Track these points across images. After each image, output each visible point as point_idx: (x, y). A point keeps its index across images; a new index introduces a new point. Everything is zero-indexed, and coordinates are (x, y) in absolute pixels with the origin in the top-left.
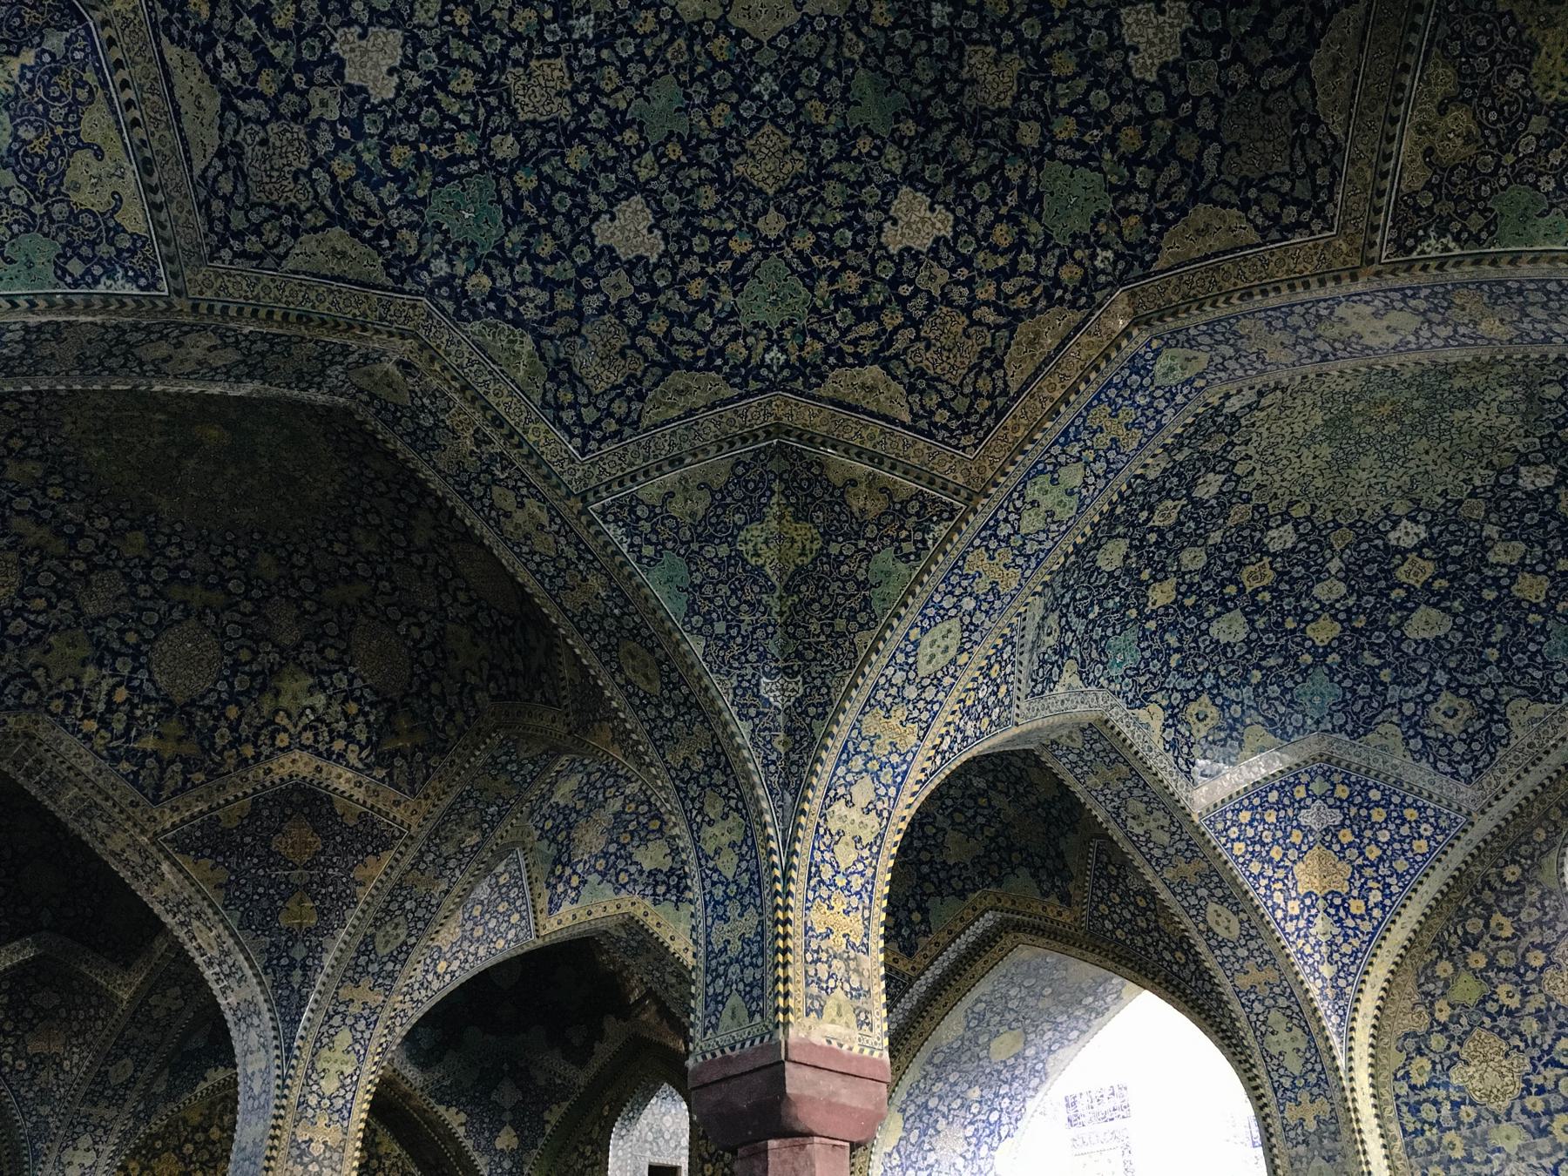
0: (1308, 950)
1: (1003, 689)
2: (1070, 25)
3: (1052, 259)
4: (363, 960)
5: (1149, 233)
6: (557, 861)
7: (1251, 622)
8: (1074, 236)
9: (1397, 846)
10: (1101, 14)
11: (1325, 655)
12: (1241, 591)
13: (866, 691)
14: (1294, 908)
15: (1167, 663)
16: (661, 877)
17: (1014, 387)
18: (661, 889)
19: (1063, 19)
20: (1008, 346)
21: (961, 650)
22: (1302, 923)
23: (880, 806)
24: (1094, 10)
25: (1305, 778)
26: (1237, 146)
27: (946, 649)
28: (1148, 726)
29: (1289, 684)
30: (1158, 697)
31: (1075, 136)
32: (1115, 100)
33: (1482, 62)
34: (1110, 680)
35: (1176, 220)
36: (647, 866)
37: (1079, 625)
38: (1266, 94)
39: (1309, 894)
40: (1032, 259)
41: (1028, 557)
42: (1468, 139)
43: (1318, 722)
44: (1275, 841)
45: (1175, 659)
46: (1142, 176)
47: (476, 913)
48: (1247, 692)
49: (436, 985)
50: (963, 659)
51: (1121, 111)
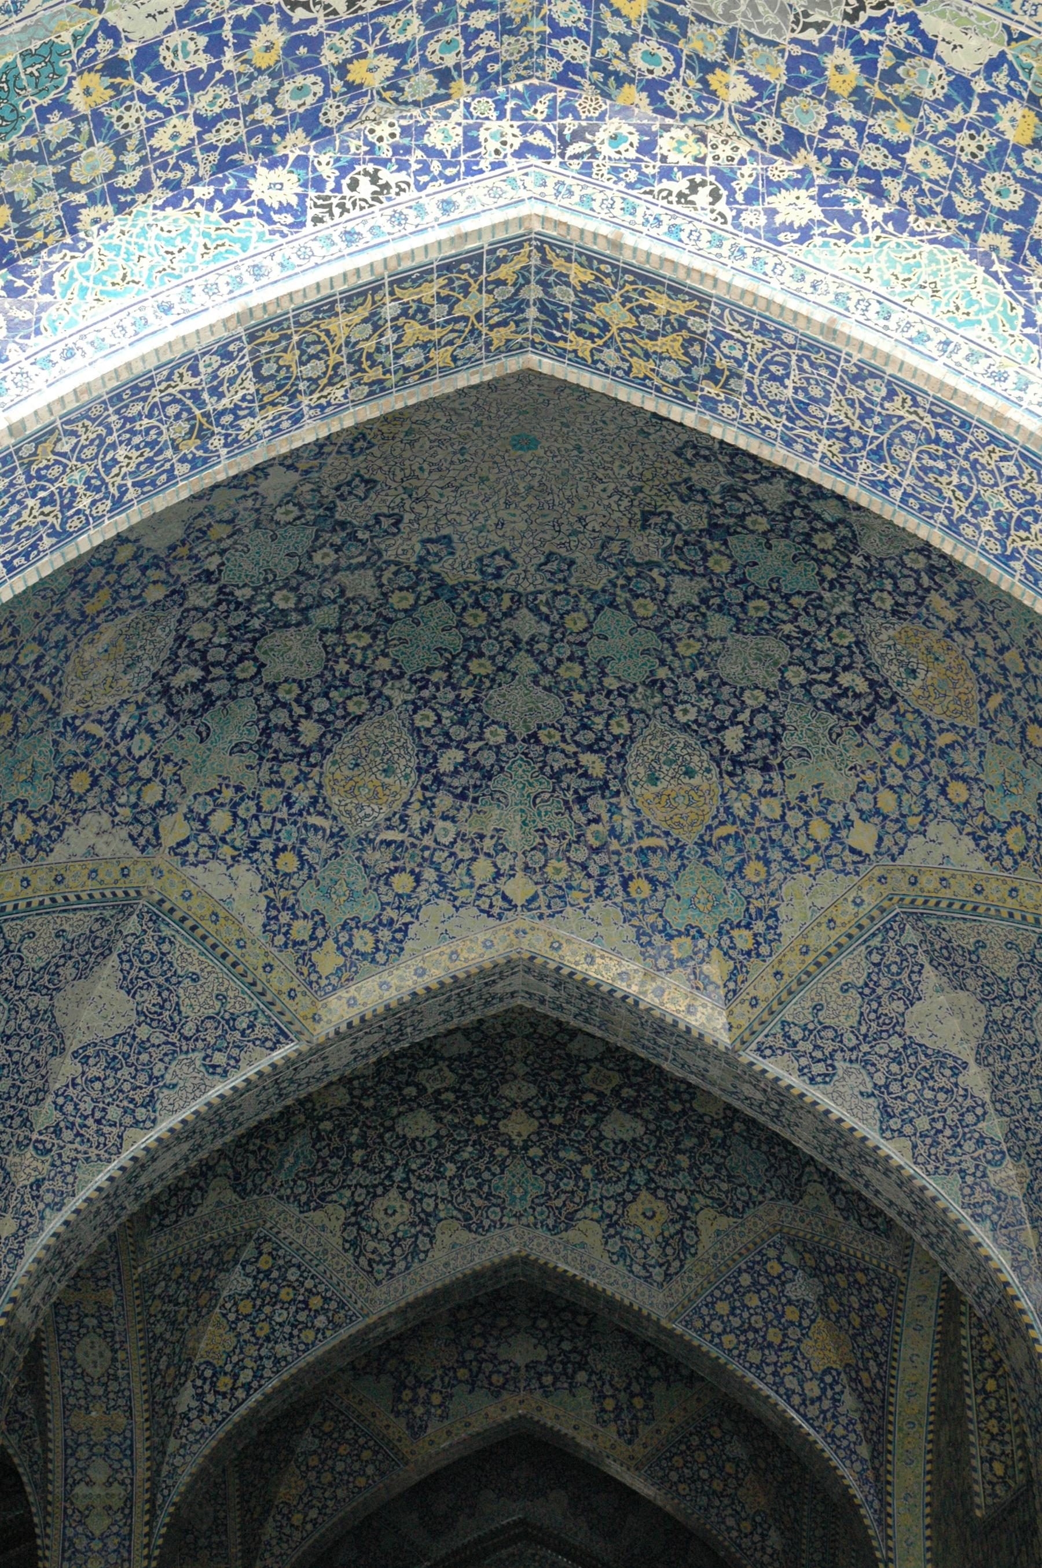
0: (840, 1431)
1: (316, 1302)
4: (190, 1538)
6: (399, 1387)
7: (638, 1116)
9: (866, 1312)
11: (730, 1125)
12: (600, 1095)
13: (59, 1401)
14: (813, 1389)
15: (579, 1177)
16: (541, 1368)
18: (548, 1380)
21: (115, 1351)
22: (826, 1404)
23: (119, 1477)
25: (772, 1253)
27: (101, 1355)
28: (583, 1245)
29: (718, 1160)
30: (588, 1211)
34: (518, 1216)
36: (520, 1360)
37: (441, 1188)
39: (827, 1371)
41: (107, 1279)
43: (762, 1192)
44: (768, 1324)
45: (587, 1171)
47: (313, 1461)
48: (683, 1178)
49: (297, 1536)
50: (121, 1355)
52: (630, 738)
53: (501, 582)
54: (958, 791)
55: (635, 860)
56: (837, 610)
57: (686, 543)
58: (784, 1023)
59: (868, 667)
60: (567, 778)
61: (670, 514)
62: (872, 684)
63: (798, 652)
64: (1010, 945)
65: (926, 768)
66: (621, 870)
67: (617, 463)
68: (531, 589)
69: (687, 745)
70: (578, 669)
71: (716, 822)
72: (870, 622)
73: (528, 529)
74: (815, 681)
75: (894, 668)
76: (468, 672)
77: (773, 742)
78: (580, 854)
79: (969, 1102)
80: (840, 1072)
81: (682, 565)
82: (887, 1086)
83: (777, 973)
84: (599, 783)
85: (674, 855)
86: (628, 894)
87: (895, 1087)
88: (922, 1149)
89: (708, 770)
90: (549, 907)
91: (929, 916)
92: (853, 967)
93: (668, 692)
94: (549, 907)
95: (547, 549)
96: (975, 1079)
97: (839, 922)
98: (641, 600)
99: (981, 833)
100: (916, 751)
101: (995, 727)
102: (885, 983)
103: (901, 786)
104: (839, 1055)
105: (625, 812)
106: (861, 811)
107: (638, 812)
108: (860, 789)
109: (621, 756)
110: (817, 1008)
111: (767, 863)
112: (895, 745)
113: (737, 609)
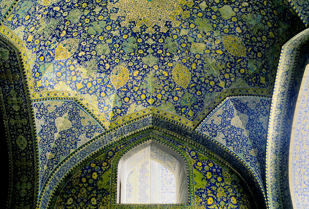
52: (73, 37)
53: (109, 2)
54: (103, 94)
55: (46, 53)
56: (123, 58)
57: (128, 30)
58: (43, 103)
59: (112, 67)
60: (58, 31)
61: (135, 26)
62: (109, 69)
63: (109, 55)
64: (90, 122)
65: (101, 87)
66: (43, 53)
67: (148, 15)
68: (108, 8)
69: (76, 47)
70: (161, 51)
71: (62, 61)
72: (123, 64)
73: (124, 4)
74: (103, 60)
75: (115, 71)
76: (82, 3)
77: (85, 61)
78: (42, 44)
79: (52, 138)
80: (42, 119)
81: (122, 31)
82: (45, 127)
83: (48, 94)
84: (59, 37)
85: (51, 59)
86: (40, 57)
87: (46, 128)
88: (41, 141)
89: (72, 53)
90: (30, 46)
91: (79, 106)
92: (59, 104)
93: (88, 39)
94: (30, 46)
95: (120, 8)
96: (57, 136)
97: (64, 95)
98: (110, 27)
99: (101, 103)
100: (102, 83)
101: (120, 92)
102: (60, 110)
103: (94, 85)
104: (44, 116)
105: (55, 45)
106: (83, 82)
107: (56, 47)
108: (87, 79)
109: (67, 37)
110: (49, 105)
111: (62, 75)
112: (100, 79)
113: (115, 43)
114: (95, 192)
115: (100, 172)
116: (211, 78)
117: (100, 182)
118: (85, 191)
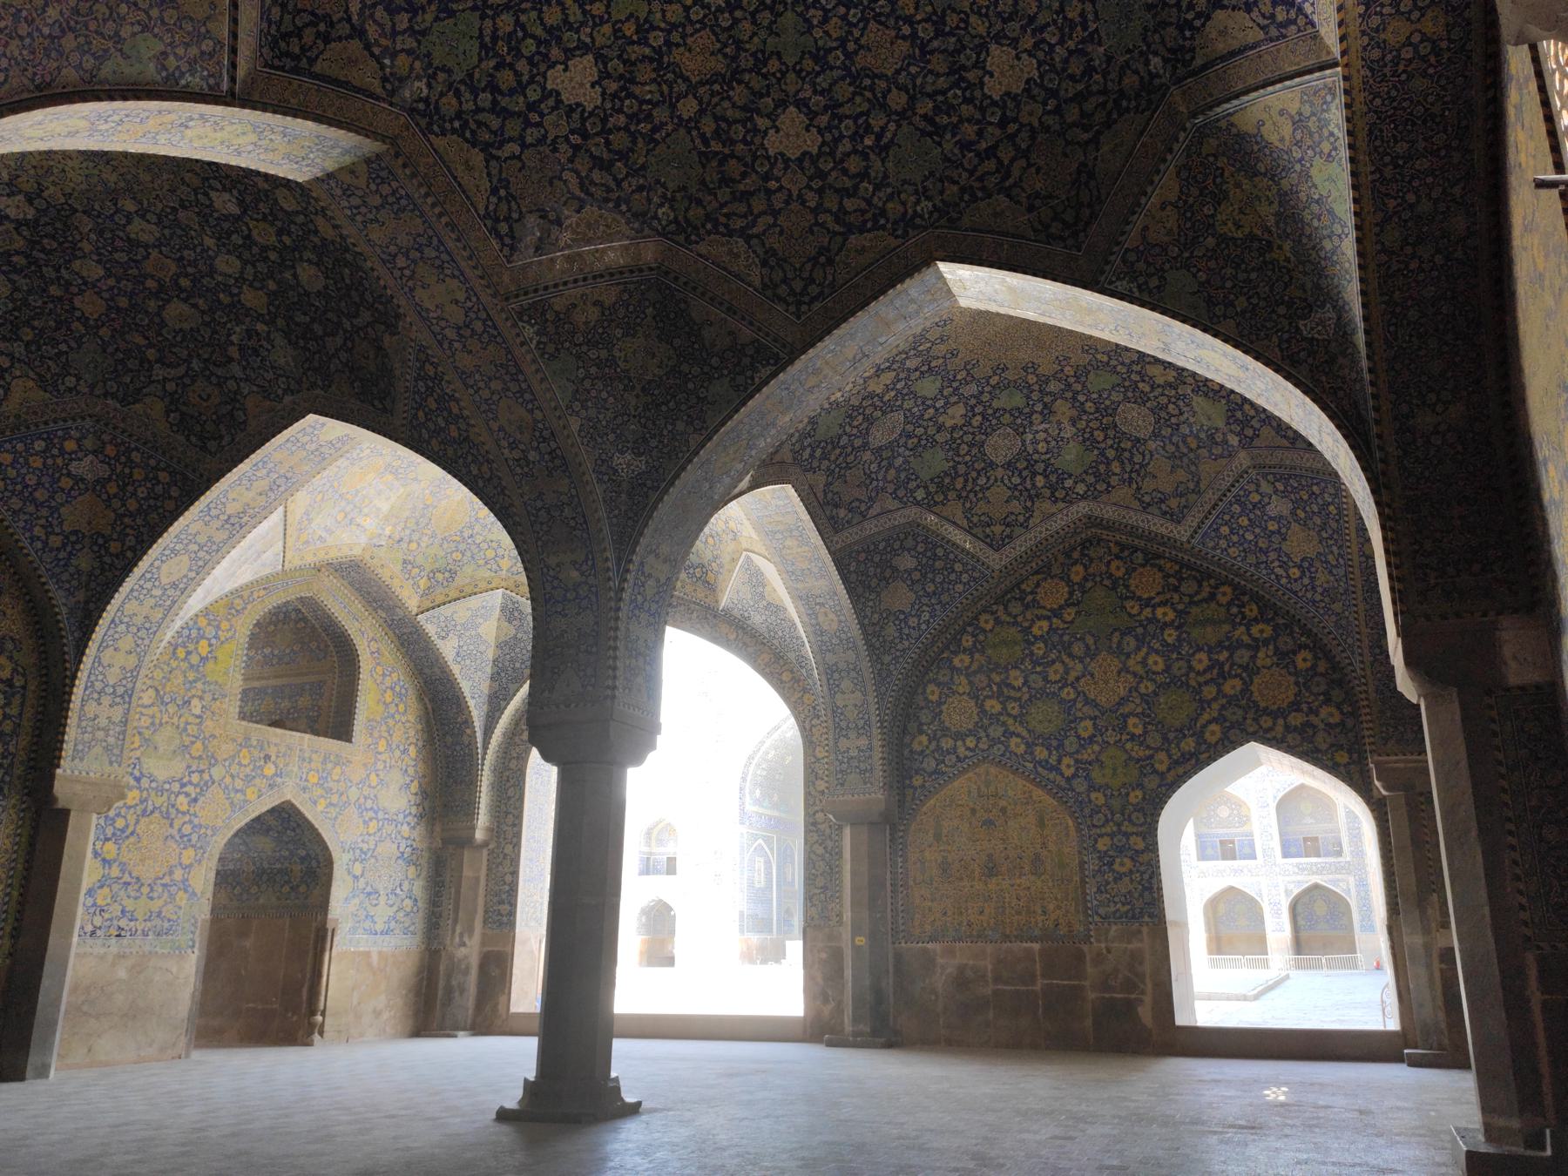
2: (580, 17)
3: (410, 43)
5: (451, 121)
8: (428, 55)
10: (588, 40)
17: (317, 68)
19: (584, 12)
20: (340, 39)
24: (591, 35)
26: (523, 167)
31: (500, 33)
32: (530, 60)
33: (622, 312)
35: (467, 141)
38: (560, 179)
40: (405, 25)
42: (586, 323)
46: (485, 98)
51: (522, 66)
114: (199, 685)
115: (214, 641)
116: (494, 545)
117: (210, 665)
118: (181, 679)
